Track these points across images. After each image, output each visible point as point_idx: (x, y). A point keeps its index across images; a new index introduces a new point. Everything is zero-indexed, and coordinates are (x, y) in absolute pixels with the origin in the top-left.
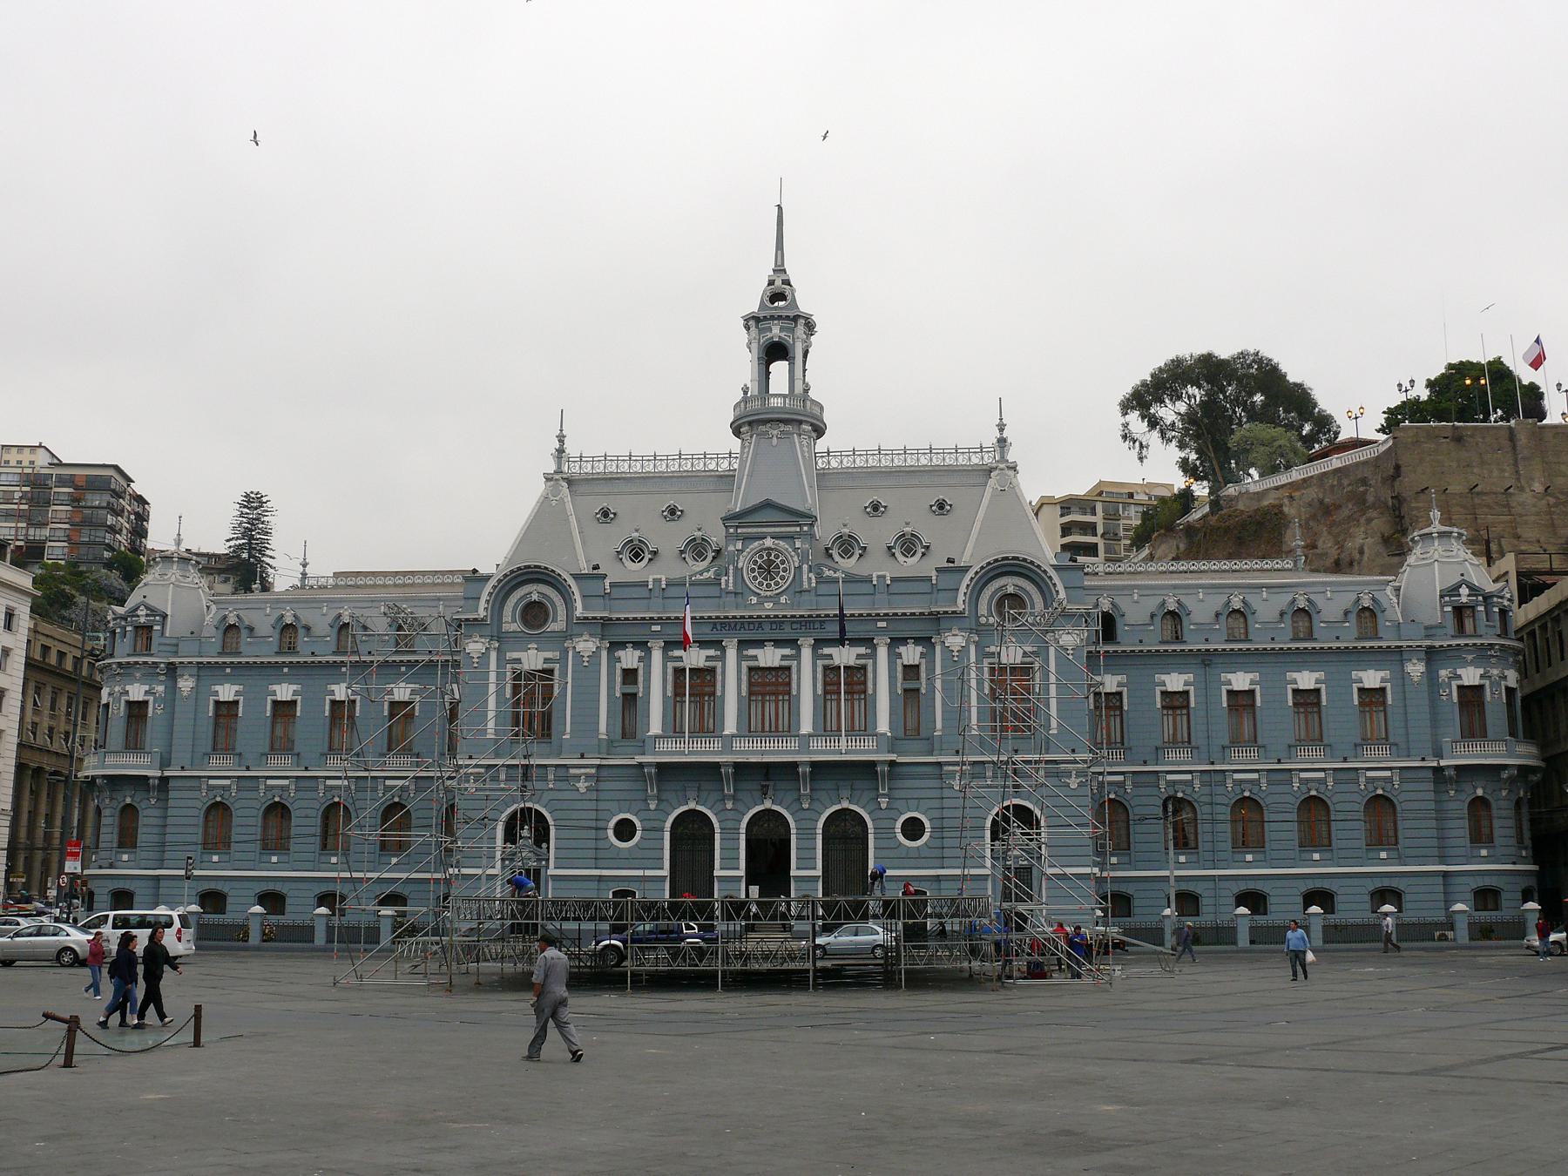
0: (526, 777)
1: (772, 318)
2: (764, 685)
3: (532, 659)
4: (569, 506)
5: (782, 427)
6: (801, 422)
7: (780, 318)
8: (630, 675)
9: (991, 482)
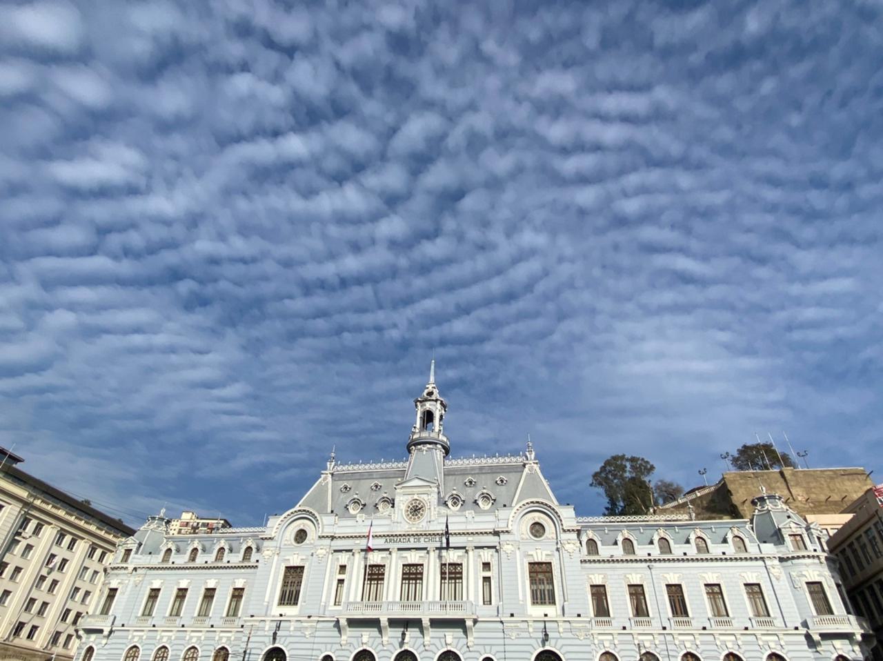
0: (278, 627)
1: (427, 400)
2: (410, 574)
3: (295, 562)
4: (330, 486)
5: (428, 446)
6: (436, 444)
7: (430, 400)
8: (343, 568)
9: (526, 470)
